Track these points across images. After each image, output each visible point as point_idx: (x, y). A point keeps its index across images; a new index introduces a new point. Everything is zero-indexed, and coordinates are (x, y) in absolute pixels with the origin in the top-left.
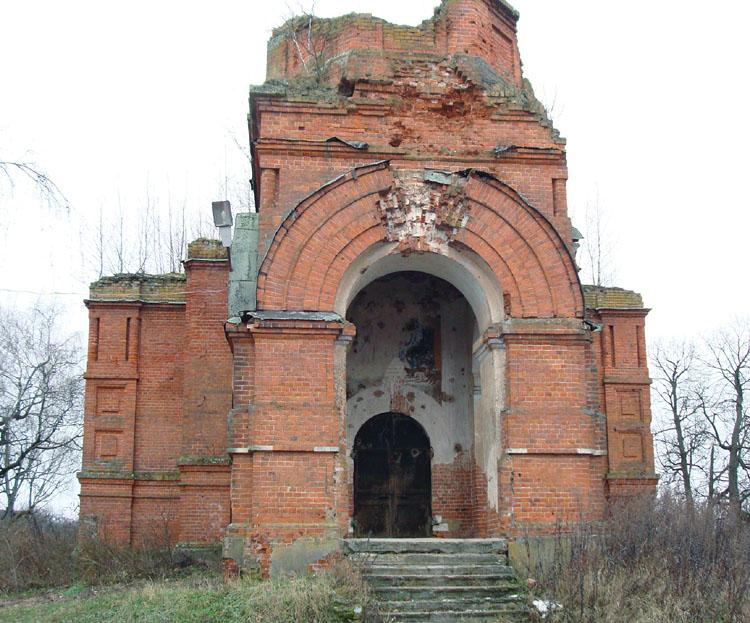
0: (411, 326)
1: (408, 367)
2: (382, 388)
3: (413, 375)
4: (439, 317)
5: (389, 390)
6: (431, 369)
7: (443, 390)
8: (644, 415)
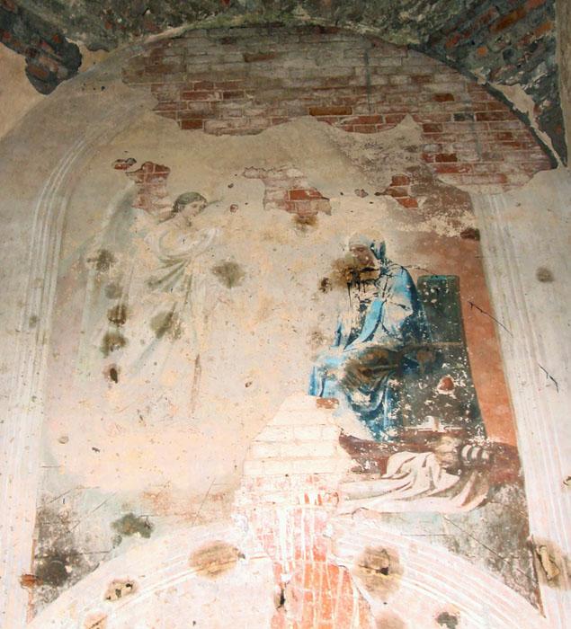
0: (359, 272)
1: (361, 432)
2: (233, 534)
3: (382, 466)
4: (472, 234)
5: (268, 539)
6: (464, 436)
7: (537, 532)
8: (564, 139)
